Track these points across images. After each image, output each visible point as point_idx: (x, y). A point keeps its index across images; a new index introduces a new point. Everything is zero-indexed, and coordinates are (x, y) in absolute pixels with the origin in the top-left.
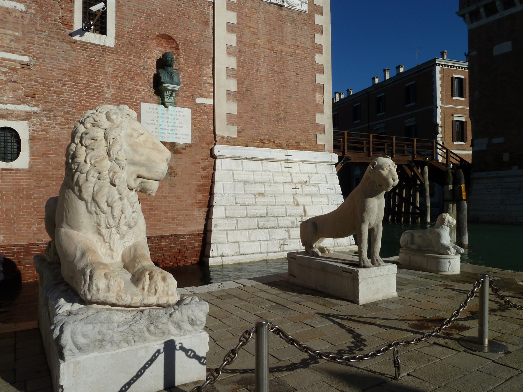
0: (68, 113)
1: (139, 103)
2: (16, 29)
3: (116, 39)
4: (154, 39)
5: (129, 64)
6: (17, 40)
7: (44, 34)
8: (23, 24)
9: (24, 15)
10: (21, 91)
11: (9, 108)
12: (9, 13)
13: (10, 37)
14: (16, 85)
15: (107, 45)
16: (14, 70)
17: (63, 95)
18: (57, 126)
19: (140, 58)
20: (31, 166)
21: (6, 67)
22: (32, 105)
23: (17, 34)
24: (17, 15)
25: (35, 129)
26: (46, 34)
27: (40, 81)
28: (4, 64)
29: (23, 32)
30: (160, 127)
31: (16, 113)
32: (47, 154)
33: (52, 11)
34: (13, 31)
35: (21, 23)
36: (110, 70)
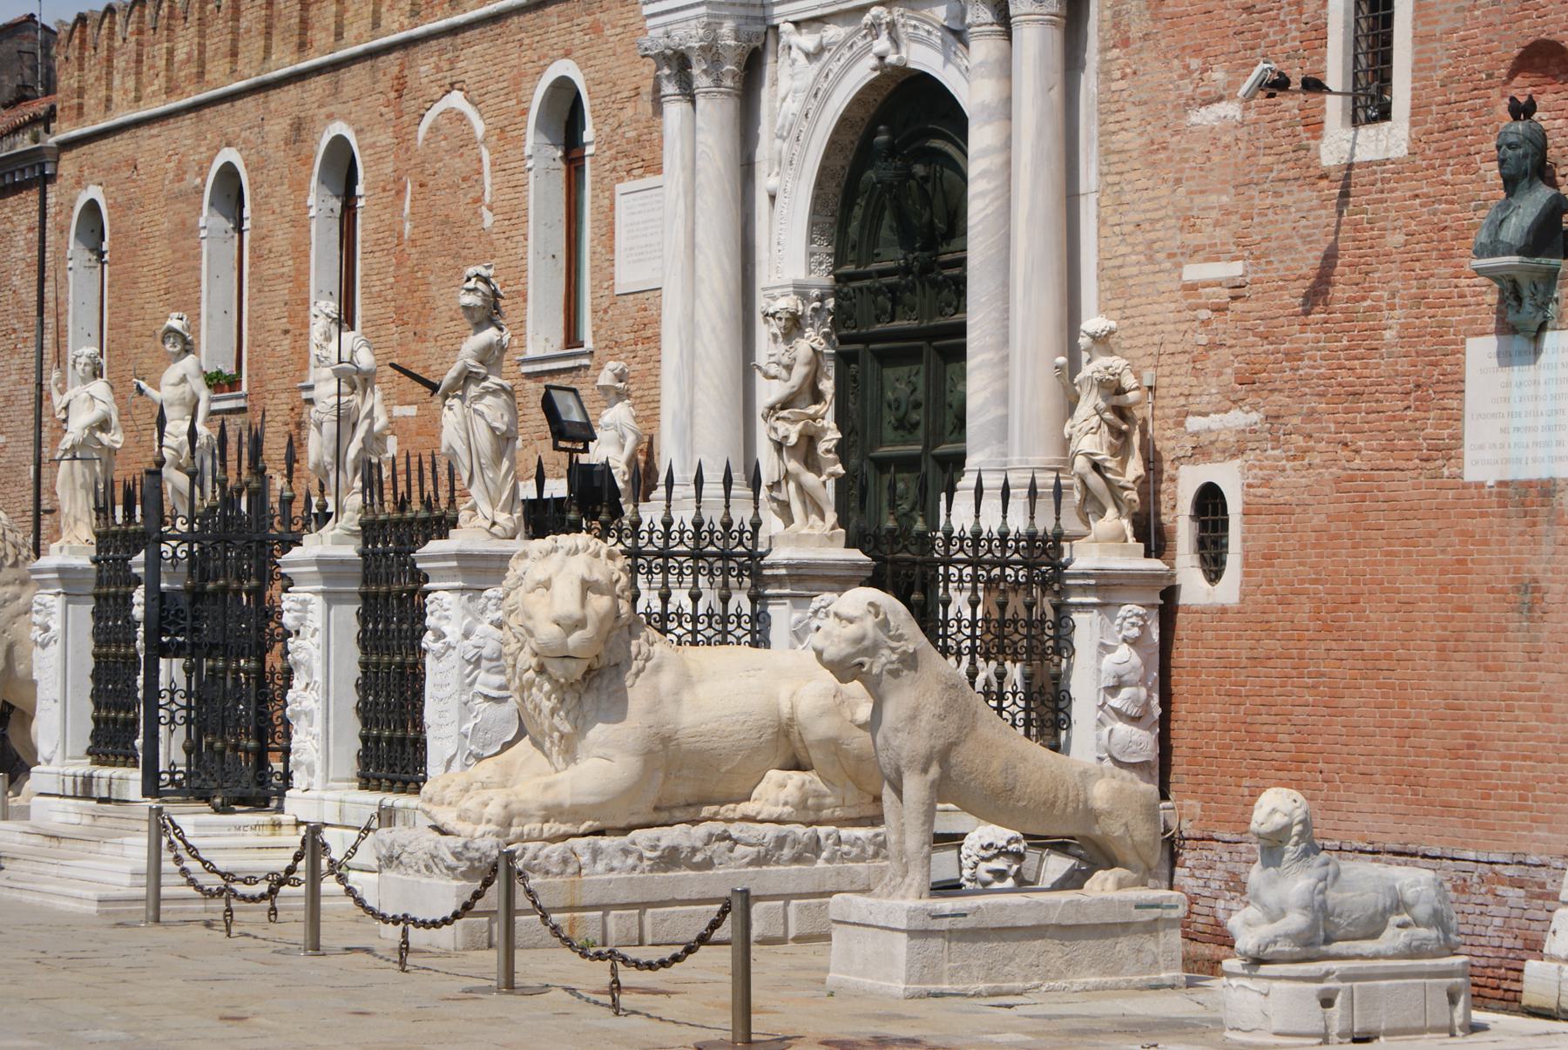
0: (1311, 415)
1: (1463, 342)
3: (1413, 124)
4: (1512, 74)
5: (1440, 202)
10: (1229, 370)
11: (1213, 427)
13: (1214, 214)
14: (1224, 353)
15: (1392, 155)
16: (1219, 309)
17: (1301, 359)
18: (1289, 465)
19: (1467, 168)
20: (1244, 595)
22: (1247, 408)
23: (1225, 199)
25: (1250, 481)
27: (1262, 329)
30: (1516, 422)
31: (1222, 437)
32: (1269, 558)
36: (1399, 238)
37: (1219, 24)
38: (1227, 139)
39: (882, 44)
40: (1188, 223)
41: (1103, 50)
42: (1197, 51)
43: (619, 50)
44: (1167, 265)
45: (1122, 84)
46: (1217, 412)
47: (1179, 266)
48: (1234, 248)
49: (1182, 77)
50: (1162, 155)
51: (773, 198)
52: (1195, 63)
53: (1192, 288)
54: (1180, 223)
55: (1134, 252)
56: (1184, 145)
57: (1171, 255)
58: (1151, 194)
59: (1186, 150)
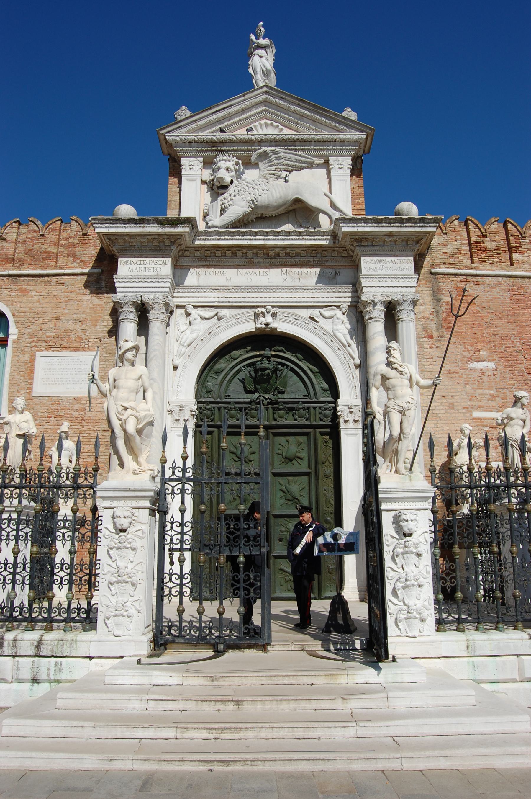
2: (490, 388)
6: (493, 397)
7: (514, 387)
8: (496, 382)
9: (495, 372)
12: (483, 373)
13: (487, 396)
21: (487, 426)
23: (492, 392)
24: (491, 373)
26: (516, 386)
28: (485, 424)
29: (496, 389)
33: (517, 363)
34: (489, 389)
35: (494, 381)
37: (483, 338)
38: (487, 374)
39: (269, 319)
40: (473, 397)
41: (418, 337)
42: (472, 345)
43: (42, 302)
44: (464, 411)
45: (429, 350)
46: (496, 461)
47: (471, 412)
48: (499, 408)
49: (464, 351)
50: (456, 375)
51: (175, 368)
52: (470, 348)
53: (480, 419)
54: (469, 398)
55: (441, 405)
56: (467, 372)
57: (464, 408)
58: (450, 387)
59: (469, 375)
